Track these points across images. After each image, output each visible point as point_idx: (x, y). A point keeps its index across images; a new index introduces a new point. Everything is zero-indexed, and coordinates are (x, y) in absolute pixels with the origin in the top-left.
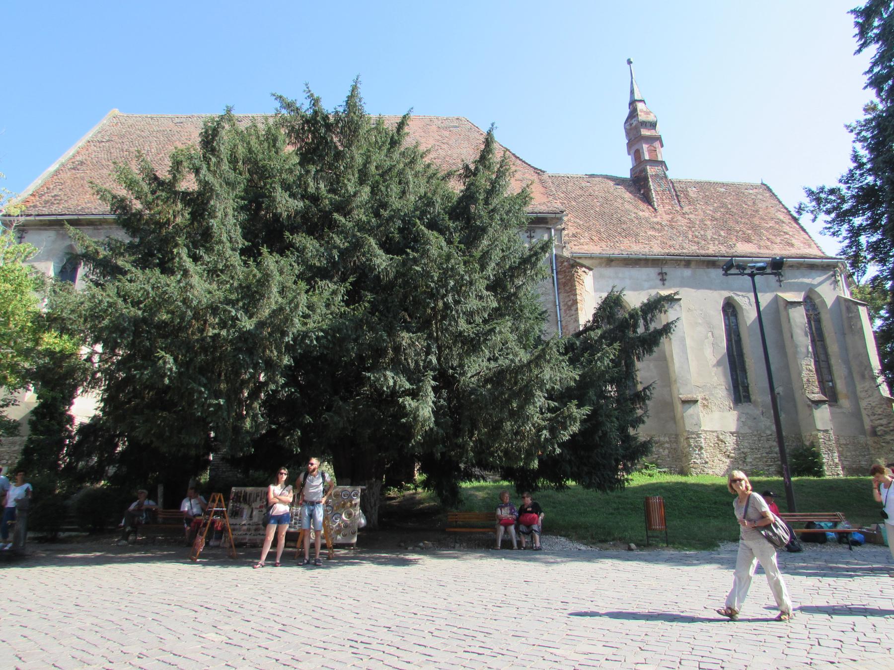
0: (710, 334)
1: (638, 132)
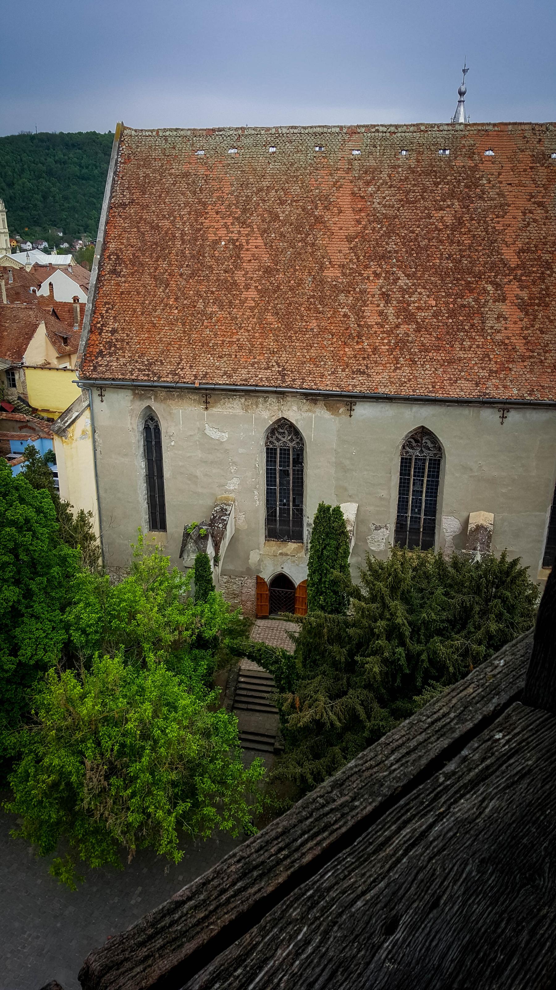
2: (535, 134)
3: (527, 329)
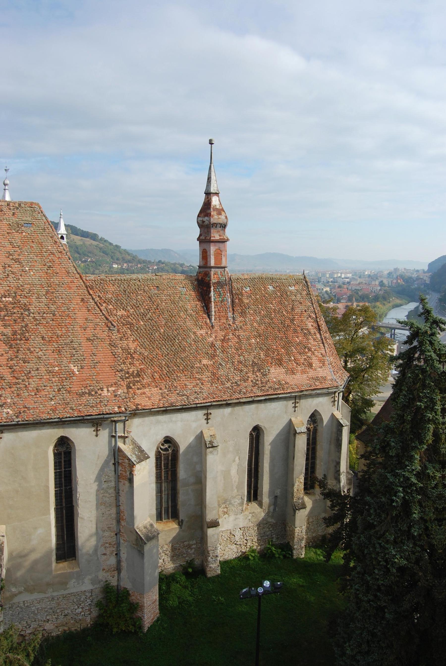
0: (237, 458)
1: (208, 224)
2: (10, 209)
3: (12, 360)
